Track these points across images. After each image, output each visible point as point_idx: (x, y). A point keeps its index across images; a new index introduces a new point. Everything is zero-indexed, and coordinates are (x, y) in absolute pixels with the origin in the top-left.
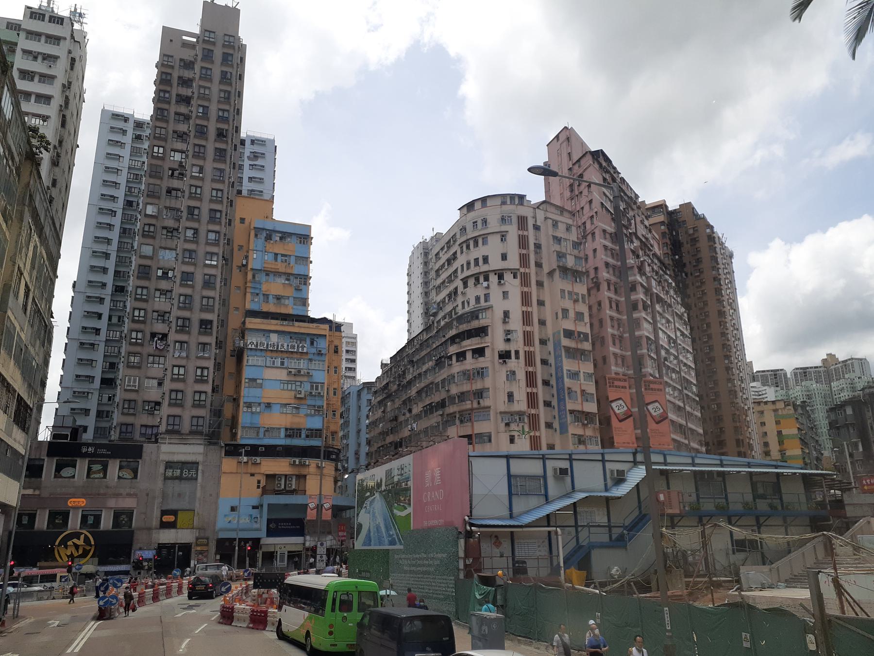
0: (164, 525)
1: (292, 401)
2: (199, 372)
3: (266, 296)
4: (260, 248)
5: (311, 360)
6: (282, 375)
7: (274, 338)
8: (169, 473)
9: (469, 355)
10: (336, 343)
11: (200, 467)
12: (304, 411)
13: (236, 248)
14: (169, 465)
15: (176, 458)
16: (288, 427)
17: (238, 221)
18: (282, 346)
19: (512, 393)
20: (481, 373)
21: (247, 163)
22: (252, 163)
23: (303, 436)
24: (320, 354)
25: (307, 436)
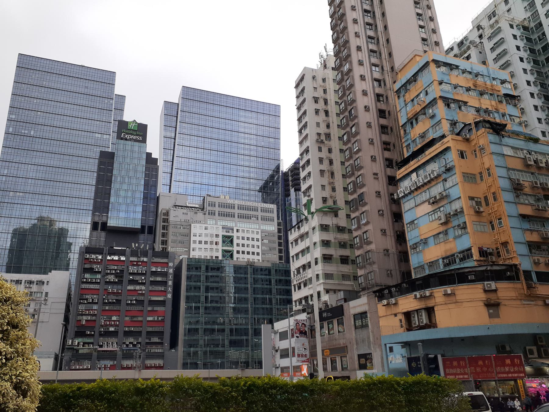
16: (444, 256)
19: (332, 160)
23: (457, 260)
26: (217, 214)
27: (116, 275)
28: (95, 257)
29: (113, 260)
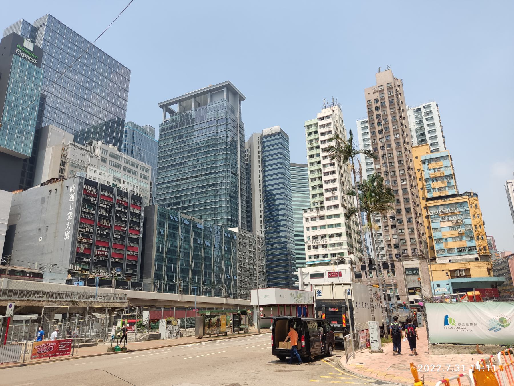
0: (411, 294)
1: (457, 235)
2: (410, 230)
3: (434, 189)
4: (426, 168)
5: (462, 215)
6: (450, 224)
7: (441, 209)
8: (407, 273)
11: (419, 270)
12: (464, 239)
13: (417, 171)
14: (407, 270)
15: (409, 267)
17: (414, 158)
18: (446, 211)
21: (424, 118)
22: (427, 117)
23: (467, 250)
25: (469, 250)
26: (108, 162)
27: (106, 210)
28: (90, 189)
29: (104, 195)
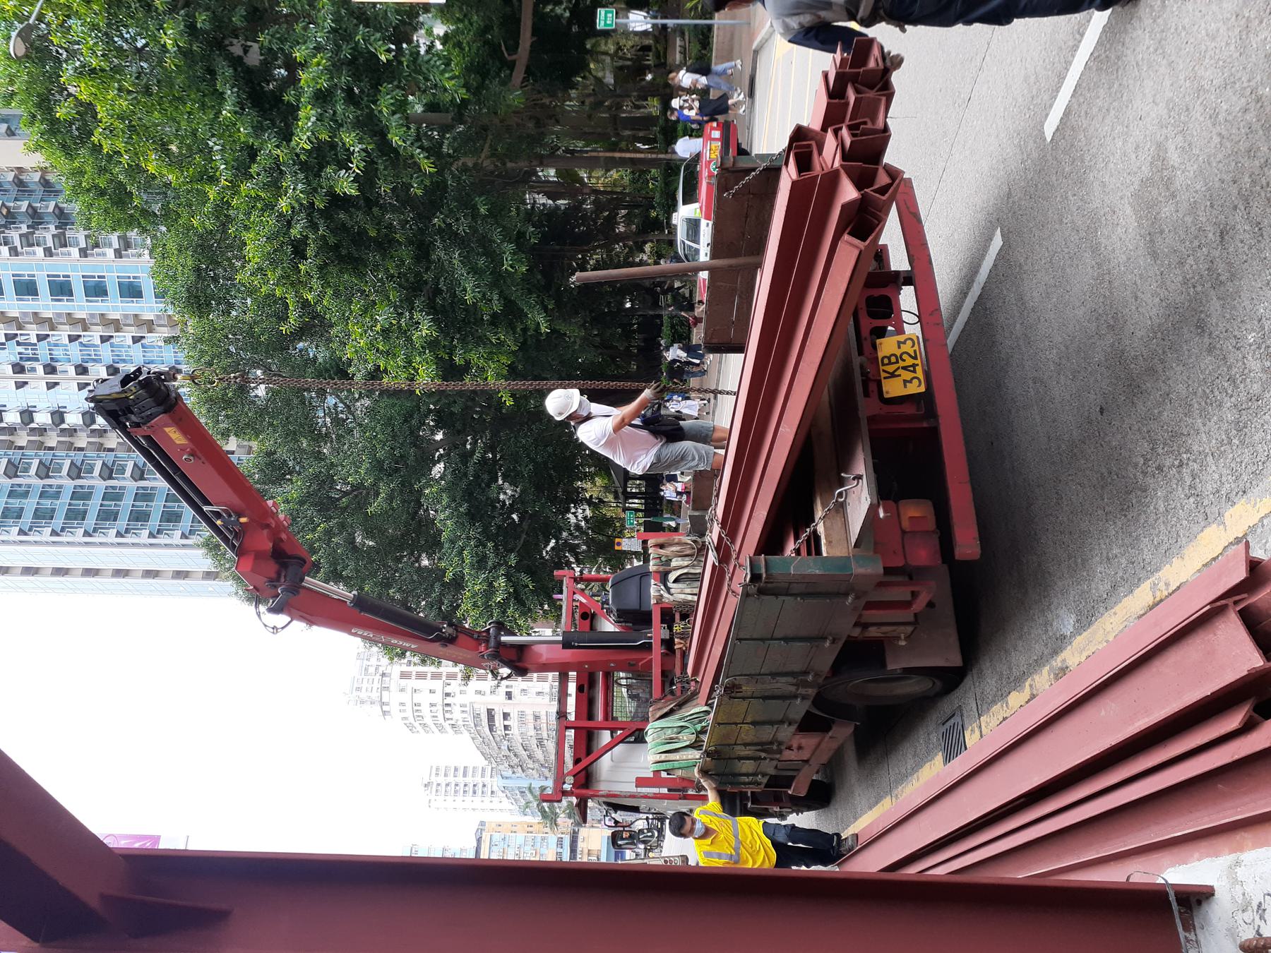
9: (506, 723)
10: (494, 825)
20: (522, 715)
24: (504, 839)
